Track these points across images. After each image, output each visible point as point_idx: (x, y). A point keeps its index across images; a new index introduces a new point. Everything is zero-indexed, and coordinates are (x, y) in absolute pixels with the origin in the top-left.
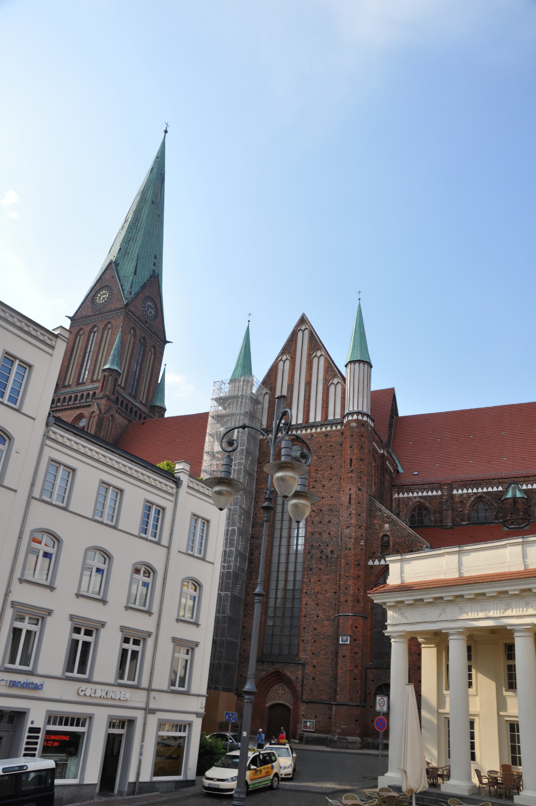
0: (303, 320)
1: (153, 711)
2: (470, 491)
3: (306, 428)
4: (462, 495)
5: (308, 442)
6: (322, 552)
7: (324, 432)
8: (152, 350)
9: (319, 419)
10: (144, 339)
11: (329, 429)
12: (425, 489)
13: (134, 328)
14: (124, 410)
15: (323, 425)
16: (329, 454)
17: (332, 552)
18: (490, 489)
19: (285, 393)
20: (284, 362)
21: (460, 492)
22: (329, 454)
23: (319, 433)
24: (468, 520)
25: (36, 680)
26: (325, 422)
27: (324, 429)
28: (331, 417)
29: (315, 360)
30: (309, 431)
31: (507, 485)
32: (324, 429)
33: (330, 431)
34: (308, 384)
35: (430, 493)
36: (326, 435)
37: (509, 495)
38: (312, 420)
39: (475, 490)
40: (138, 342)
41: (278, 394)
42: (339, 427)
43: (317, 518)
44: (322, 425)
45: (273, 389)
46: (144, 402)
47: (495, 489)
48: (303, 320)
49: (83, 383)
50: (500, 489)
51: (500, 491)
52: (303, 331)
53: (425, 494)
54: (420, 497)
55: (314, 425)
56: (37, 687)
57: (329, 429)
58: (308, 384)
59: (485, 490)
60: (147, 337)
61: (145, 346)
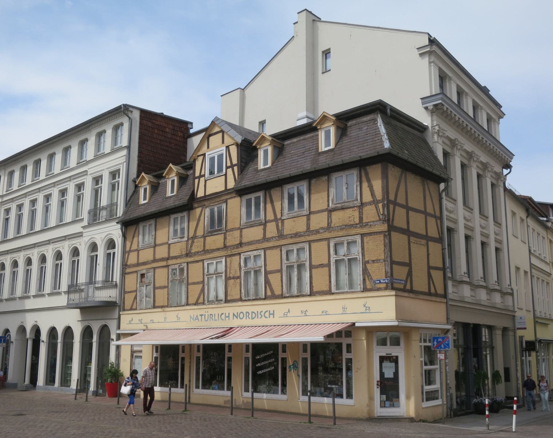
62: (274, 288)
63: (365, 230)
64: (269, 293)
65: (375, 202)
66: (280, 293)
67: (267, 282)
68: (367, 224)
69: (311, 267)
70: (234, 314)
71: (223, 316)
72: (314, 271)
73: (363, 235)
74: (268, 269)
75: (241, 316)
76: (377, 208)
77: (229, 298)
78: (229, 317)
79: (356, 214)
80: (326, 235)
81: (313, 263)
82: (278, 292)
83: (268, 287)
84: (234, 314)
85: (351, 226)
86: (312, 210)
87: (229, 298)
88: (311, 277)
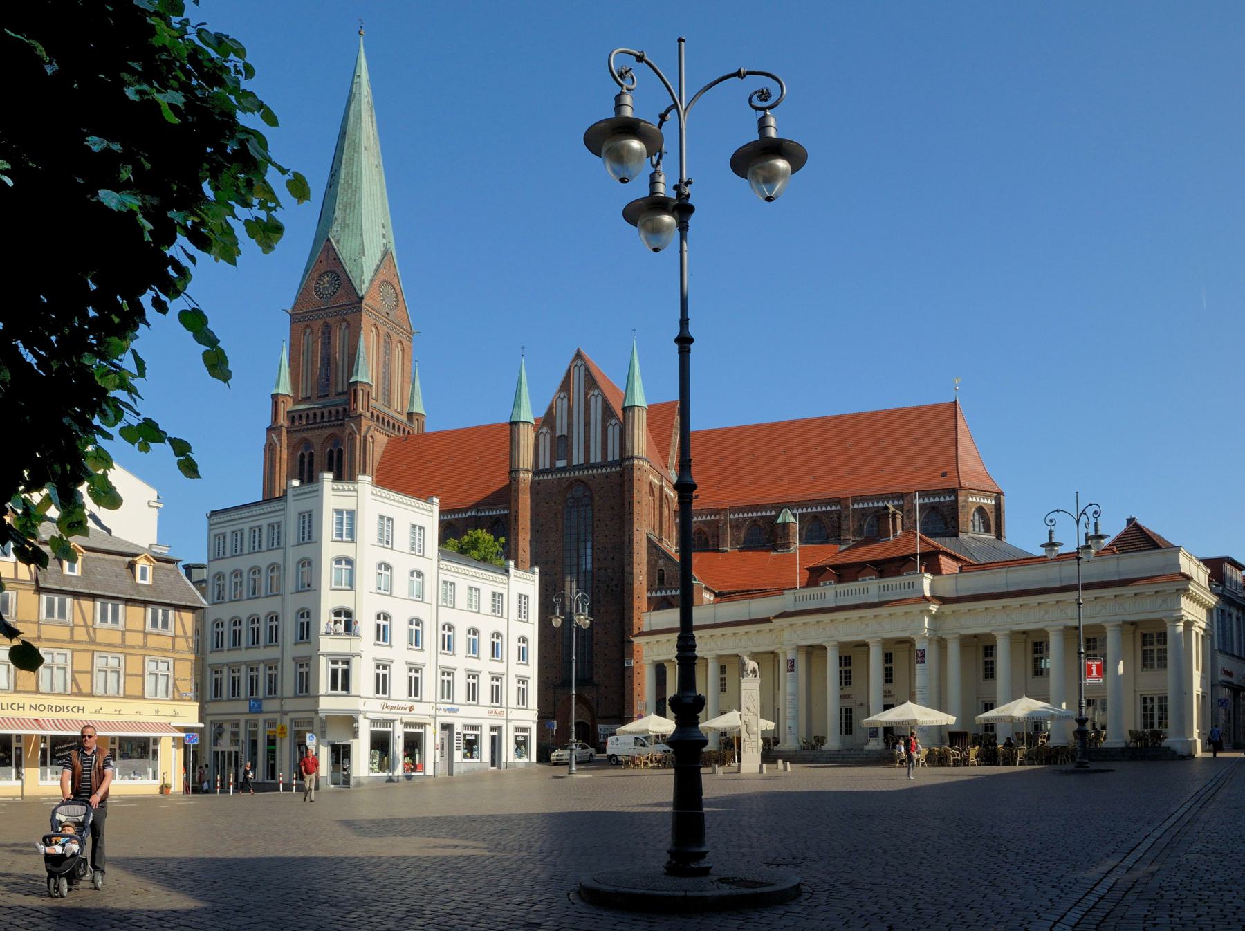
0: (579, 356)
1: (511, 720)
2: (745, 515)
3: (587, 469)
4: (738, 519)
5: (590, 483)
6: (608, 586)
7: (605, 474)
8: (399, 345)
9: (599, 460)
10: (388, 335)
11: (609, 470)
12: (704, 514)
13: (375, 326)
14: (381, 425)
15: (604, 466)
16: (610, 495)
17: (616, 585)
18: (764, 514)
19: (565, 433)
20: (562, 400)
21: (736, 516)
22: (610, 495)
23: (599, 474)
24: (743, 544)
25: (456, 707)
26: (605, 463)
27: (604, 471)
28: (610, 459)
29: (593, 398)
30: (590, 472)
31: (779, 510)
32: (604, 471)
33: (611, 472)
34: (587, 424)
35: (709, 518)
36: (607, 477)
37: (780, 520)
38: (592, 461)
39: (750, 515)
40: (382, 341)
41: (558, 434)
42: (618, 469)
43: (602, 555)
44: (602, 467)
45: (553, 428)
46: (399, 410)
47: (768, 513)
48: (579, 356)
49: (327, 395)
50: (773, 513)
51: (773, 516)
52: (579, 367)
53: (704, 518)
54: (699, 522)
55: (594, 466)
56: (455, 711)
57: (609, 470)
58: (587, 424)
59: (759, 514)
60: (390, 332)
61: (391, 342)
62: (81, 685)
63: (177, 656)
64: (75, 690)
65: (186, 637)
66: (89, 691)
67: (74, 680)
68: (178, 652)
69: (126, 675)
70: (31, 706)
71: (15, 707)
72: (127, 678)
73: (175, 659)
74: (75, 668)
75: (42, 708)
76: (187, 641)
77: (18, 688)
78: (23, 707)
79: (170, 641)
80: (142, 652)
81: (128, 672)
82: (86, 690)
83: (74, 685)
84: (31, 706)
85: (165, 650)
86: (127, 628)
87: (18, 688)
88: (125, 683)
